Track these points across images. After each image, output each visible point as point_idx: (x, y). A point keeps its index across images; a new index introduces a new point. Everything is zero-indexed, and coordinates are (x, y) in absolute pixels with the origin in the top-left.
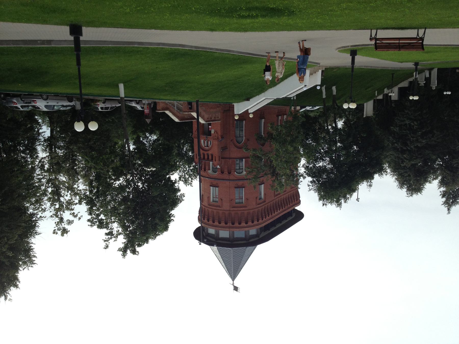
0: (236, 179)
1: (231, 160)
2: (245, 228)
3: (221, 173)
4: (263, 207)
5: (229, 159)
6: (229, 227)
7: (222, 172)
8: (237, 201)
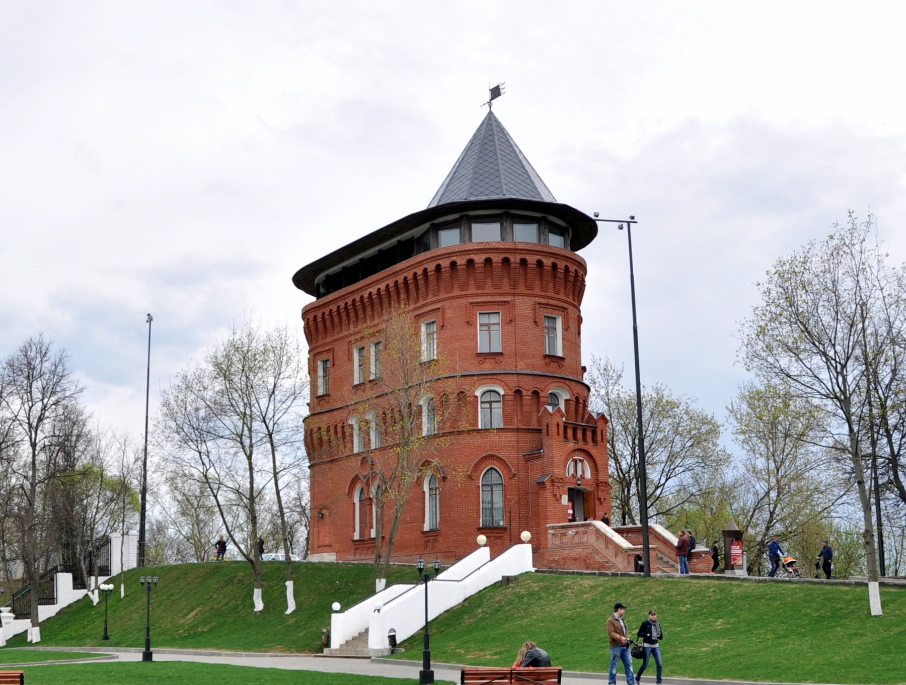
0: (499, 377)
1: (516, 427)
2: (474, 250)
3: (538, 390)
4: (421, 303)
5: (519, 427)
6: (515, 251)
7: (536, 393)
8: (494, 319)
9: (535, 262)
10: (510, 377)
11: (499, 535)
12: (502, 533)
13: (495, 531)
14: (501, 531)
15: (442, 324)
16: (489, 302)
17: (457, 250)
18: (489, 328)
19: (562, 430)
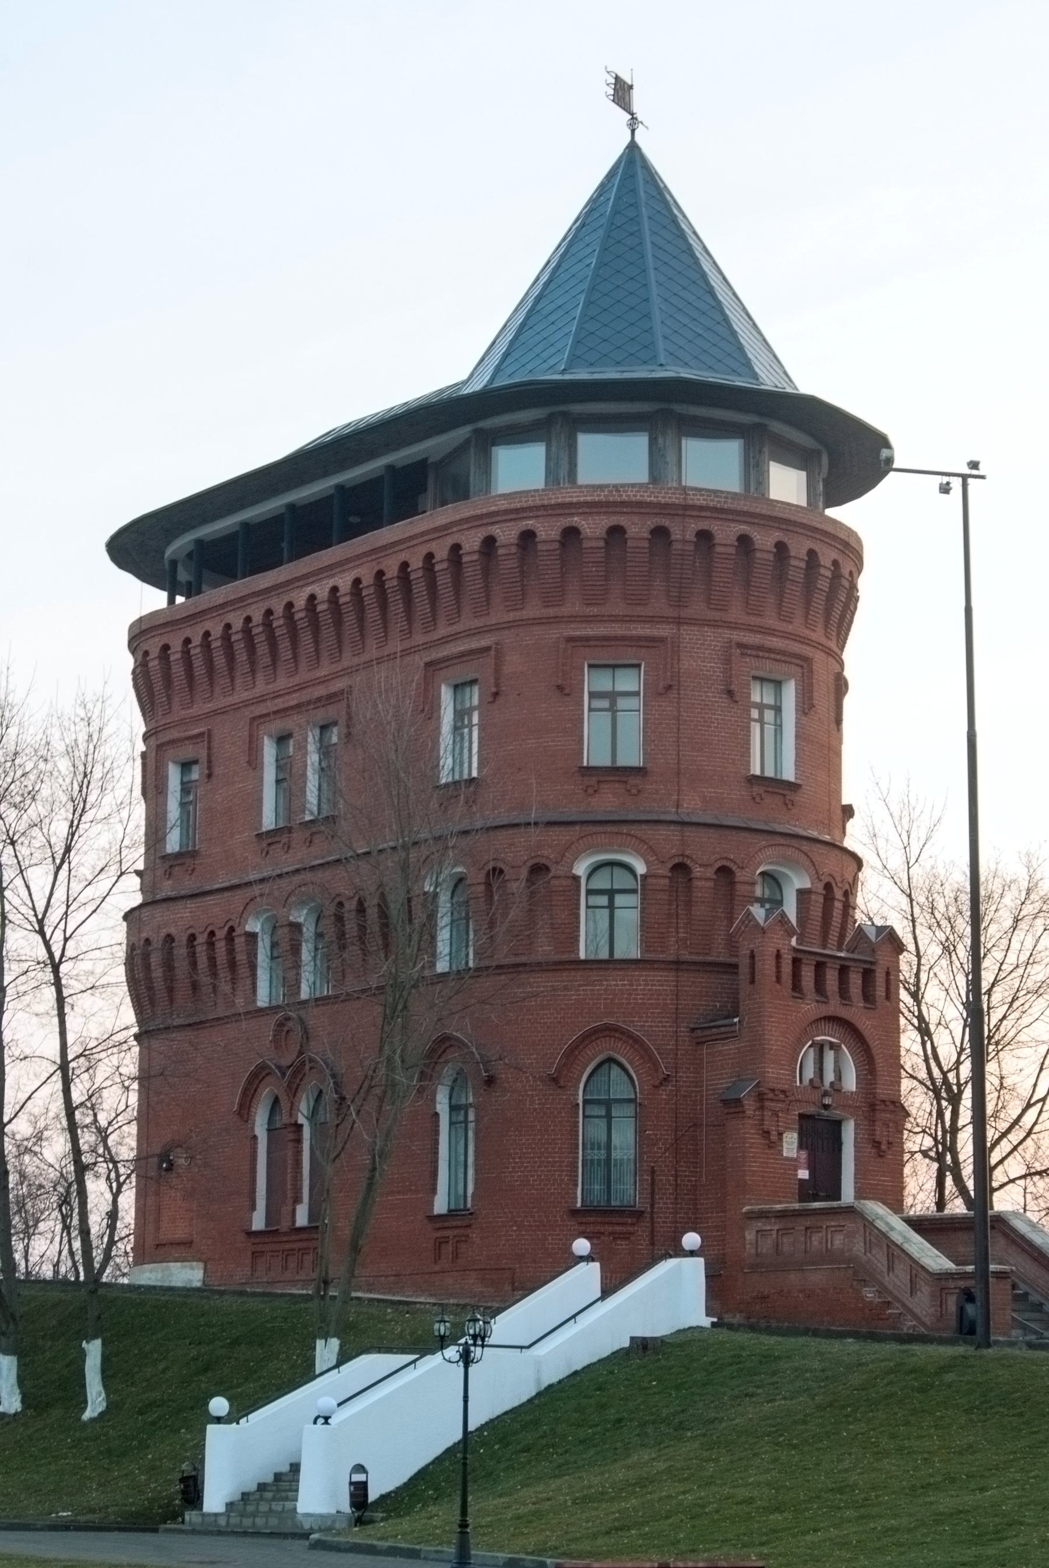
0: (635, 830)
1: (671, 958)
4: (442, 631)
5: (683, 958)
6: (684, 510)
7: (725, 872)
8: (628, 681)
9: (732, 540)
10: (663, 831)
11: (623, 1229)
12: (633, 1224)
13: (614, 1220)
14: (629, 1220)
15: (494, 690)
16: (616, 638)
17: (539, 503)
18: (613, 704)
19: (787, 969)
